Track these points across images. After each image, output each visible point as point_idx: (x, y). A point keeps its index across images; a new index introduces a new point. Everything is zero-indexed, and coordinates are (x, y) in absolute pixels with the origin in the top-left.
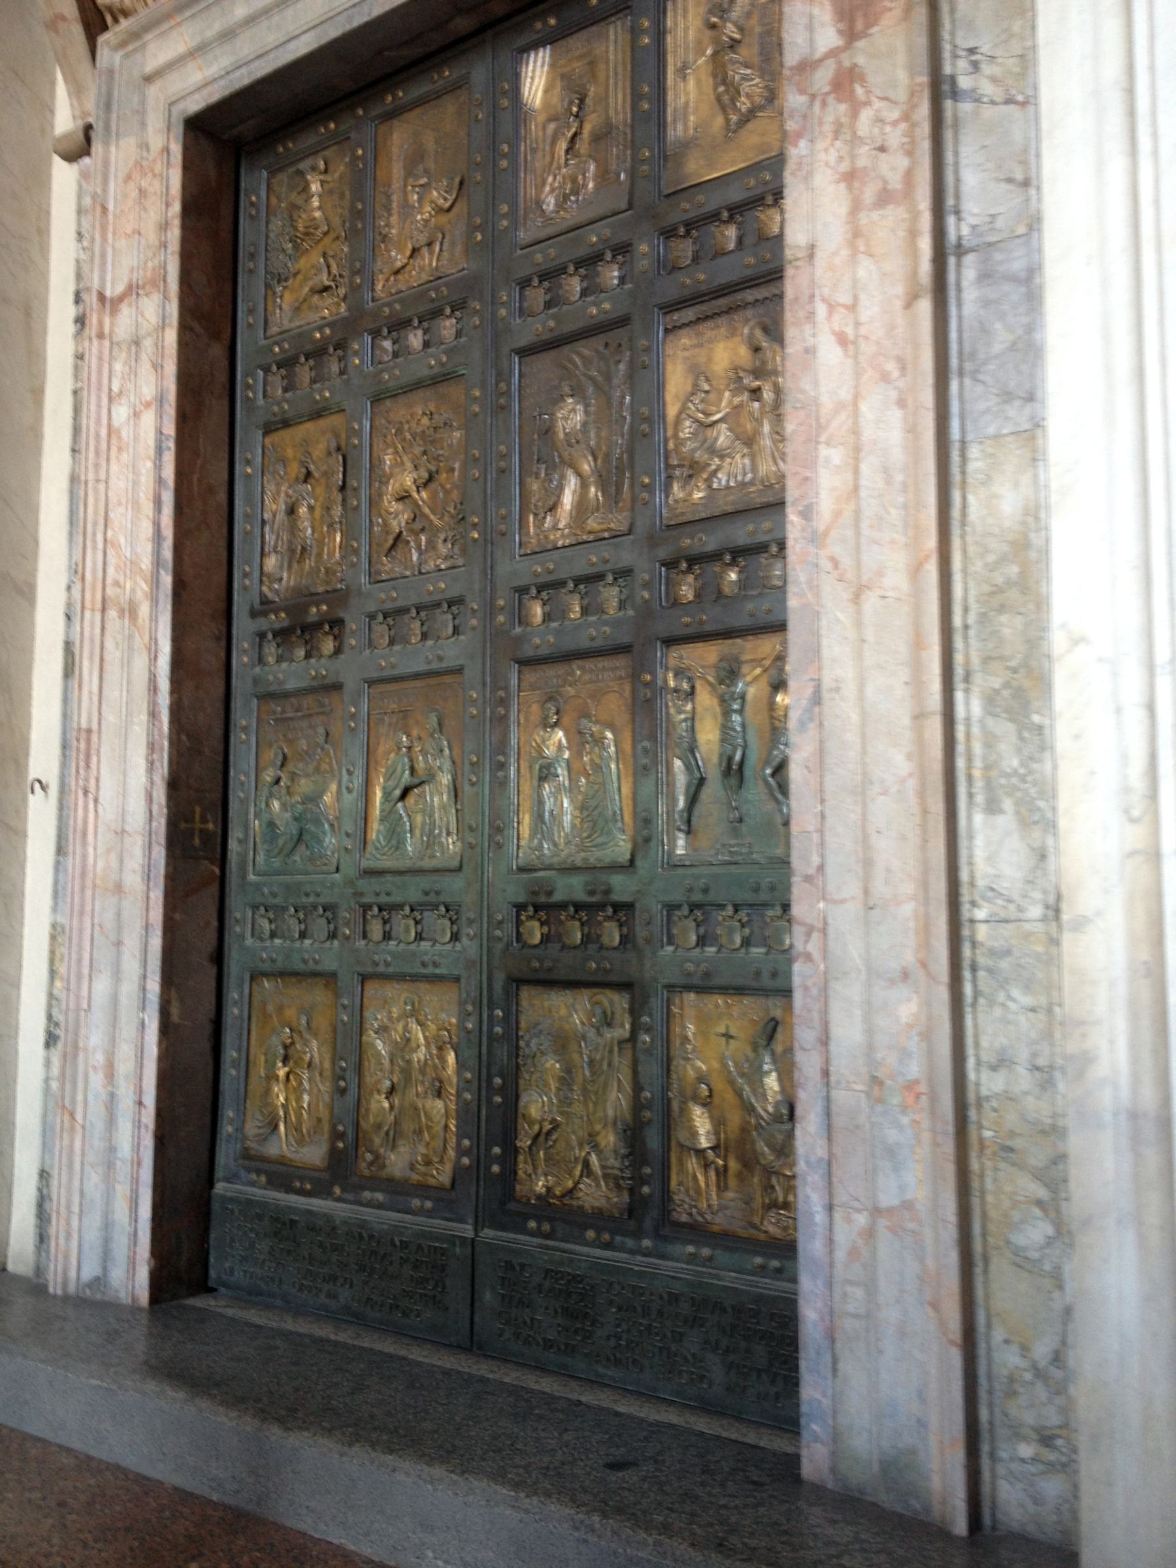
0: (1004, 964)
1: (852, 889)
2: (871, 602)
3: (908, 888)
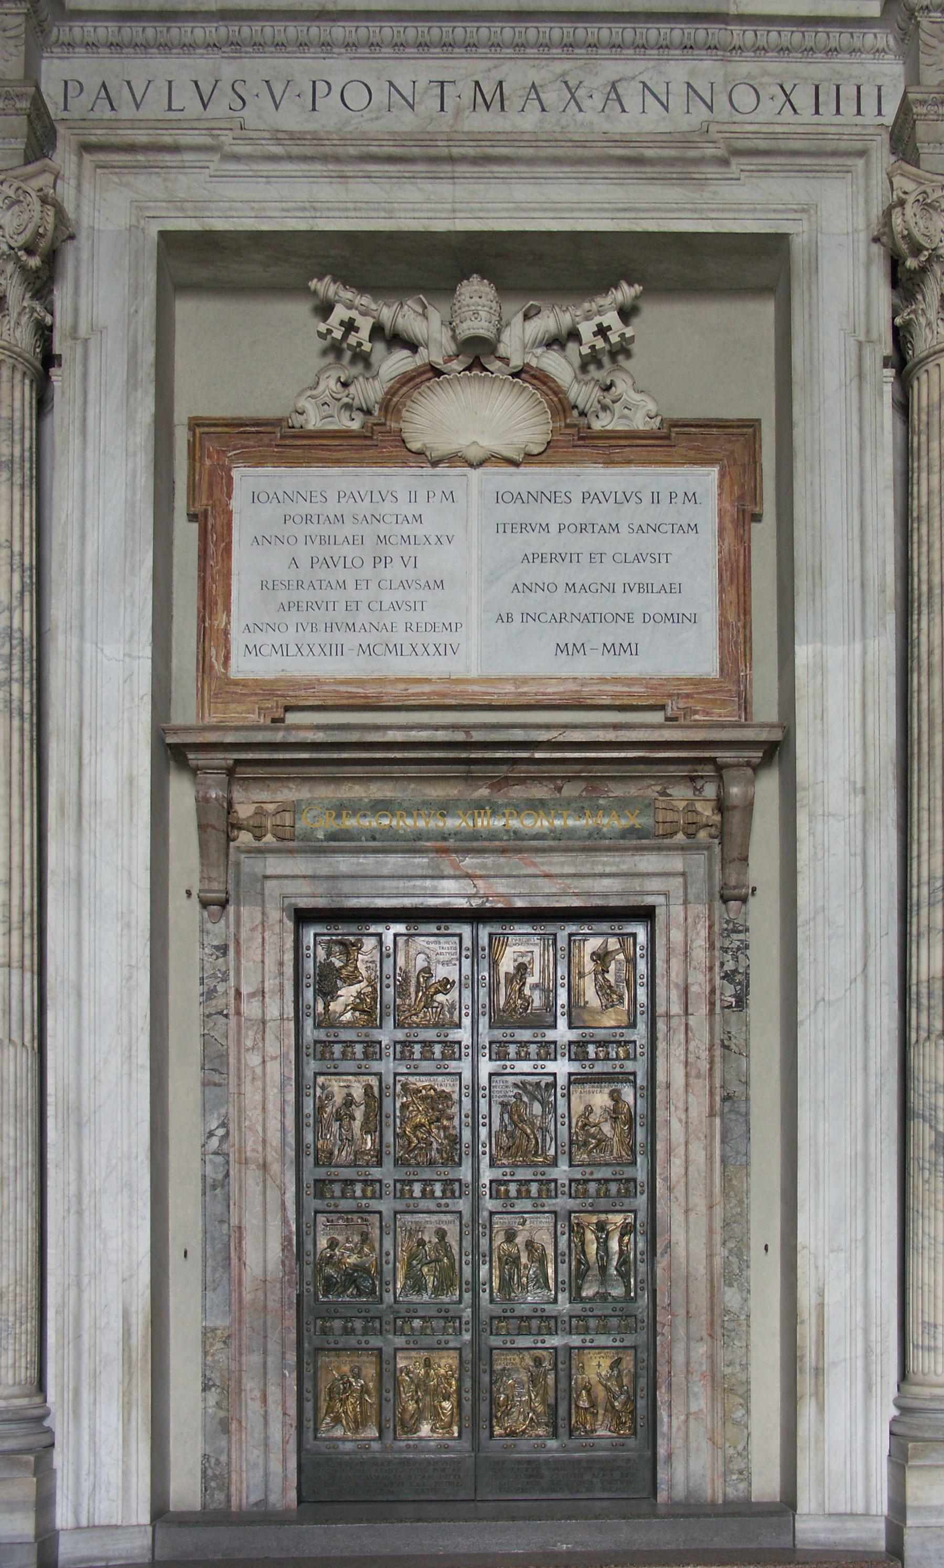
0: (733, 1334)
1: (682, 1311)
2: (692, 1216)
3: (704, 1311)
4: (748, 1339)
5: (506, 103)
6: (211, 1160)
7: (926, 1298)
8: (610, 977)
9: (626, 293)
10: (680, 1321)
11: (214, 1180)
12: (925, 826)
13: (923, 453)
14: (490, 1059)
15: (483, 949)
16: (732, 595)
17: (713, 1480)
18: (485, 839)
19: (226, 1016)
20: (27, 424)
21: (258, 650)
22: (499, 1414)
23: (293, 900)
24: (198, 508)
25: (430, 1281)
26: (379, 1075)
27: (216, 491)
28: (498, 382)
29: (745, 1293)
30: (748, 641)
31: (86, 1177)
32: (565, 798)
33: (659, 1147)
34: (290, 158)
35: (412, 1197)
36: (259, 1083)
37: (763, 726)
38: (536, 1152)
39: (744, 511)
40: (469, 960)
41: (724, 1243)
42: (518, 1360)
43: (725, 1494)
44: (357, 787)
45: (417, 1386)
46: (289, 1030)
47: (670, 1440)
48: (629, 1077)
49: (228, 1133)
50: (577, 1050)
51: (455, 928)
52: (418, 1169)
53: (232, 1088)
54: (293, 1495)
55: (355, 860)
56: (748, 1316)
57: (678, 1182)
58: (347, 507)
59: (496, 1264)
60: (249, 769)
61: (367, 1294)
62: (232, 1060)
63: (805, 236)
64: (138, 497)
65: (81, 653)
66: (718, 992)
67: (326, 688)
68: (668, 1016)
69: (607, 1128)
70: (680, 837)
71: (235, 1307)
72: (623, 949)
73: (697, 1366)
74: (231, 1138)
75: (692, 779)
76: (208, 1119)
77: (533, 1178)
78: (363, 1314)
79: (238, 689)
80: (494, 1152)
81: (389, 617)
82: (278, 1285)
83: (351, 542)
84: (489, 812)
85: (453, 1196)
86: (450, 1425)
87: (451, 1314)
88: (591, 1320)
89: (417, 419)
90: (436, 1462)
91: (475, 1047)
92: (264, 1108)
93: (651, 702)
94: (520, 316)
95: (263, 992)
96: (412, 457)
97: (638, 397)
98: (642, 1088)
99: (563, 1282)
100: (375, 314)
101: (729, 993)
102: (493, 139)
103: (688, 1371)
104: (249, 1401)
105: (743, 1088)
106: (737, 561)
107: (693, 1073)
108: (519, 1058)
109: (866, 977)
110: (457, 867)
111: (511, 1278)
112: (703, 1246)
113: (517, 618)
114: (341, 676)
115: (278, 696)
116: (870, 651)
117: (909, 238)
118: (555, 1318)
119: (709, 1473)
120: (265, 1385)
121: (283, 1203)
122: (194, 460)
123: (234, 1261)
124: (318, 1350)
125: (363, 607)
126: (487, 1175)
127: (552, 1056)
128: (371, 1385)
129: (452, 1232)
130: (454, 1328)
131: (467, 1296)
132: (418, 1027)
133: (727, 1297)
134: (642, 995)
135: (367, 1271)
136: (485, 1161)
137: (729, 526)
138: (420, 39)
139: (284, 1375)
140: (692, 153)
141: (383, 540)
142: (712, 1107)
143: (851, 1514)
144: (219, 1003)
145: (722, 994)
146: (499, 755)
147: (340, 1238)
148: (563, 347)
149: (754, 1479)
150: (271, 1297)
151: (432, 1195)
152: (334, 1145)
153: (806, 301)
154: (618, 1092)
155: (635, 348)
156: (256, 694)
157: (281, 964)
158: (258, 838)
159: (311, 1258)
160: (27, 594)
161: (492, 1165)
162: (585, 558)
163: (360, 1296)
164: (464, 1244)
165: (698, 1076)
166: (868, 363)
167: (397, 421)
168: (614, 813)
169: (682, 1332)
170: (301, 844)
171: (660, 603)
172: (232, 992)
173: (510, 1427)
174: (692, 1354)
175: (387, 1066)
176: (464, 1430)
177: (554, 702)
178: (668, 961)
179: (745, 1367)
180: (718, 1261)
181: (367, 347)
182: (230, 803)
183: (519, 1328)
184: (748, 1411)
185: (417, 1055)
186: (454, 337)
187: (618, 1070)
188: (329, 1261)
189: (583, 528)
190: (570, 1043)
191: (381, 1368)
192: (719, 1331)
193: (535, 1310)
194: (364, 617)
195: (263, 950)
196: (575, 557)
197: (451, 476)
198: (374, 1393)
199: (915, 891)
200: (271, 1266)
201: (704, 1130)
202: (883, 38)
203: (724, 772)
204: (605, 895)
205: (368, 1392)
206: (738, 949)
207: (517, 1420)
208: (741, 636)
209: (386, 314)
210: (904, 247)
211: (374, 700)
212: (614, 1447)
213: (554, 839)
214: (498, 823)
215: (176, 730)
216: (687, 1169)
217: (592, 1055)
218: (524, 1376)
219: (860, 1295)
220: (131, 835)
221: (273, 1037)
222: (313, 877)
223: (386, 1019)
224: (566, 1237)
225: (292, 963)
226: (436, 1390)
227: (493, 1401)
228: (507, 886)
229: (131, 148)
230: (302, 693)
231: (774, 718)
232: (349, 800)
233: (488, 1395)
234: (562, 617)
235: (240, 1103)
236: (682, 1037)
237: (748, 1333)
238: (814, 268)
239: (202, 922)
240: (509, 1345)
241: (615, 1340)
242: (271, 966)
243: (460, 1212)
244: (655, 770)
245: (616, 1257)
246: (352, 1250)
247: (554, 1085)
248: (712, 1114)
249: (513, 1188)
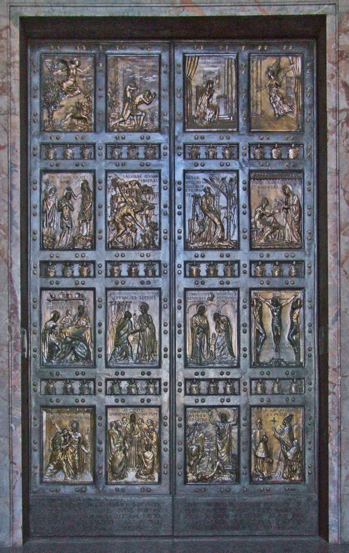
35: (120, 276)
52: (125, 252)
69: (281, 219)
80: (187, 238)
85: (154, 275)
99: (245, 350)
129: (153, 304)
132: (125, 131)
136: (180, 244)
139: (11, 429)
151: (137, 275)
152: (56, 232)
159: (37, 329)
161: (186, 248)
191: (95, 422)
249: (203, 268)
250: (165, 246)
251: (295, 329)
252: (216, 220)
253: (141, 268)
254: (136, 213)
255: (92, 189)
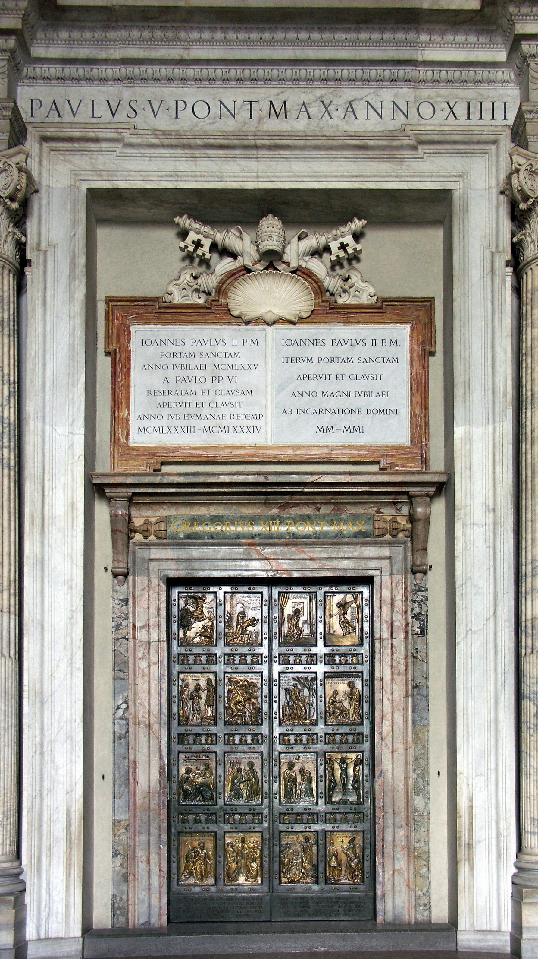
0: (420, 823)
1: (390, 810)
2: (396, 755)
3: (403, 810)
4: (428, 827)
5: (288, 114)
6: (118, 723)
7: (532, 804)
8: (348, 617)
9: (357, 224)
10: (389, 816)
11: (120, 734)
12: (529, 531)
13: (529, 316)
14: (279, 664)
15: (275, 601)
16: (418, 398)
17: (409, 910)
18: (276, 538)
19: (127, 639)
20: (11, 299)
21: (145, 430)
22: (285, 870)
23: (166, 573)
24: (111, 349)
25: (245, 792)
26: (215, 673)
27: (121, 339)
28: (283, 277)
29: (426, 800)
30: (427, 424)
31: (46, 733)
32: (322, 514)
33: (376, 714)
34: (163, 146)
35: (234, 744)
36: (146, 678)
37: (435, 473)
38: (306, 717)
39: (425, 350)
40: (267, 607)
41: (414, 771)
42: (295, 839)
43: (416, 918)
44: (202, 508)
45: (237, 854)
46: (163, 647)
47: (383, 886)
48: (359, 675)
49: (128, 707)
50: (329, 659)
51: (259, 589)
52: (237, 727)
53: (131, 681)
54: (165, 918)
55: (201, 550)
56: (429, 813)
57: (387, 735)
58: (197, 348)
59: (282, 782)
60: (140, 498)
61: (208, 800)
62: (131, 665)
63: (461, 191)
64: (76, 342)
65: (44, 431)
66: (410, 625)
67: (185, 452)
68: (381, 639)
69: (346, 704)
70: (388, 537)
71: (132, 808)
72: (355, 600)
73: (399, 842)
74: (130, 710)
75: (395, 503)
76: (117, 698)
77: (304, 732)
78: (206, 812)
79: (134, 452)
81: (221, 411)
82: (157, 795)
83: (199, 368)
84: (278, 522)
85: (258, 743)
86: (256, 877)
87: (257, 811)
88: (337, 815)
89: (237, 298)
90: (248, 898)
91: (271, 657)
92: (149, 692)
93: (371, 459)
94: (296, 238)
95: (149, 625)
96: (234, 320)
97: (364, 285)
98: (366, 681)
99: (321, 793)
100: (213, 237)
101: (416, 626)
102: (280, 135)
103: (394, 845)
104: (140, 863)
105: (425, 681)
106: (421, 379)
107: (396, 672)
108: (296, 664)
109: (496, 617)
110: (260, 554)
111: (291, 790)
112: (402, 772)
113: (294, 411)
114: (193, 445)
115: (157, 456)
116: (498, 430)
117: (521, 191)
118: (317, 814)
119: (407, 906)
120: (149, 853)
121: (160, 747)
122: (109, 321)
123: (132, 781)
124: (180, 833)
125: (206, 405)
126: (277, 731)
127: (315, 662)
128: (210, 853)
129: (257, 763)
130: (259, 820)
131: (266, 801)
132: (238, 645)
133: (416, 802)
134: (366, 627)
135: (208, 786)
136: (276, 722)
137: (416, 358)
138: (238, 76)
139: (160, 848)
140: (395, 143)
141: (217, 367)
142: (407, 692)
143: (490, 931)
144: (123, 632)
145: (412, 627)
146: (284, 490)
147: (193, 767)
148: (321, 256)
149: (433, 909)
150: (153, 802)
151: (246, 742)
152: (189, 713)
153: (461, 229)
154: (353, 683)
155: (362, 256)
156: (145, 455)
157: (159, 609)
158: (146, 537)
159: (176, 779)
160: (12, 398)
161: (280, 725)
162: (333, 377)
163: (204, 801)
164: (264, 770)
165: (399, 674)
166: (497, 265)
167: (225, 299)
168: (350, 523)
169: (390, 822)
170: (170, 541)
171: (377, 403)
172: (131, 626)
173: (291, 878)
174: (396, 835)
175: (220, 668)
176: (264, 879)
177: (315, 460)
178: (381, 608)
179: (427, 843)
180: (411, 781)
181: (208, 256)
182: (130, 518)
183: (296, 819)
184: (429, 869)
185: (237, 662)
186: (258, 250)
187: (352, 670)
188: (186, 780)
189: (332, 360)
190: (325, 654)
191: (216, 843)
192: (412, 822)
193: (305, 809)
194: (206, 411)
195: (149, 601)
196: (327, 377)
197: (256, 330)
198: (212, 858)
199: (524, 568)
200: (152, 784)
201: (402, 705)
202: (508, 74)
203: (413, 499)
204: (345, 570)
205: (208, 857)
206: (422, 601)
207: (295, 874)
208: (423, 422)
209: (219, 237)
210: (518, 196)
211: (212, 458)
212: (352, 890)
213: (315, 538)
214: (283, 529)
215: (99, 476)
216: (392, 727)
217: (338, 662)
218: (299, 847)
219: (493, 802)
220: (72, 536)
221: (154, 651)
222: (178, 560)
223: (219, 641)
224: (323, 766)
225: (165, 609)
226: (248, 856)
227: (281, 862)
228: (289, 565)
229: (71, 140)
230: (171, 454)
231: (442, 468)
232: (198, 515)
233: (278, 859)
234: (320, 411)
235: (135, 690)
236: (390, 651)
237: (428, 823)
238: (466, 209)
239: (114, 585)
240: (290, 830)
241: (351, 827)
242: (153, 611)
243: (262, 752)
244: (374, 499)
245: (352, 778)
246: (199, 774)
247: (316, 679)
248: (407, 696)
249: (292, 738)
250: (266, 723)
251: (356, 780)
252: (301, 705)
253: (249, 739)
254: (245, 701)
255: (214, 684)
